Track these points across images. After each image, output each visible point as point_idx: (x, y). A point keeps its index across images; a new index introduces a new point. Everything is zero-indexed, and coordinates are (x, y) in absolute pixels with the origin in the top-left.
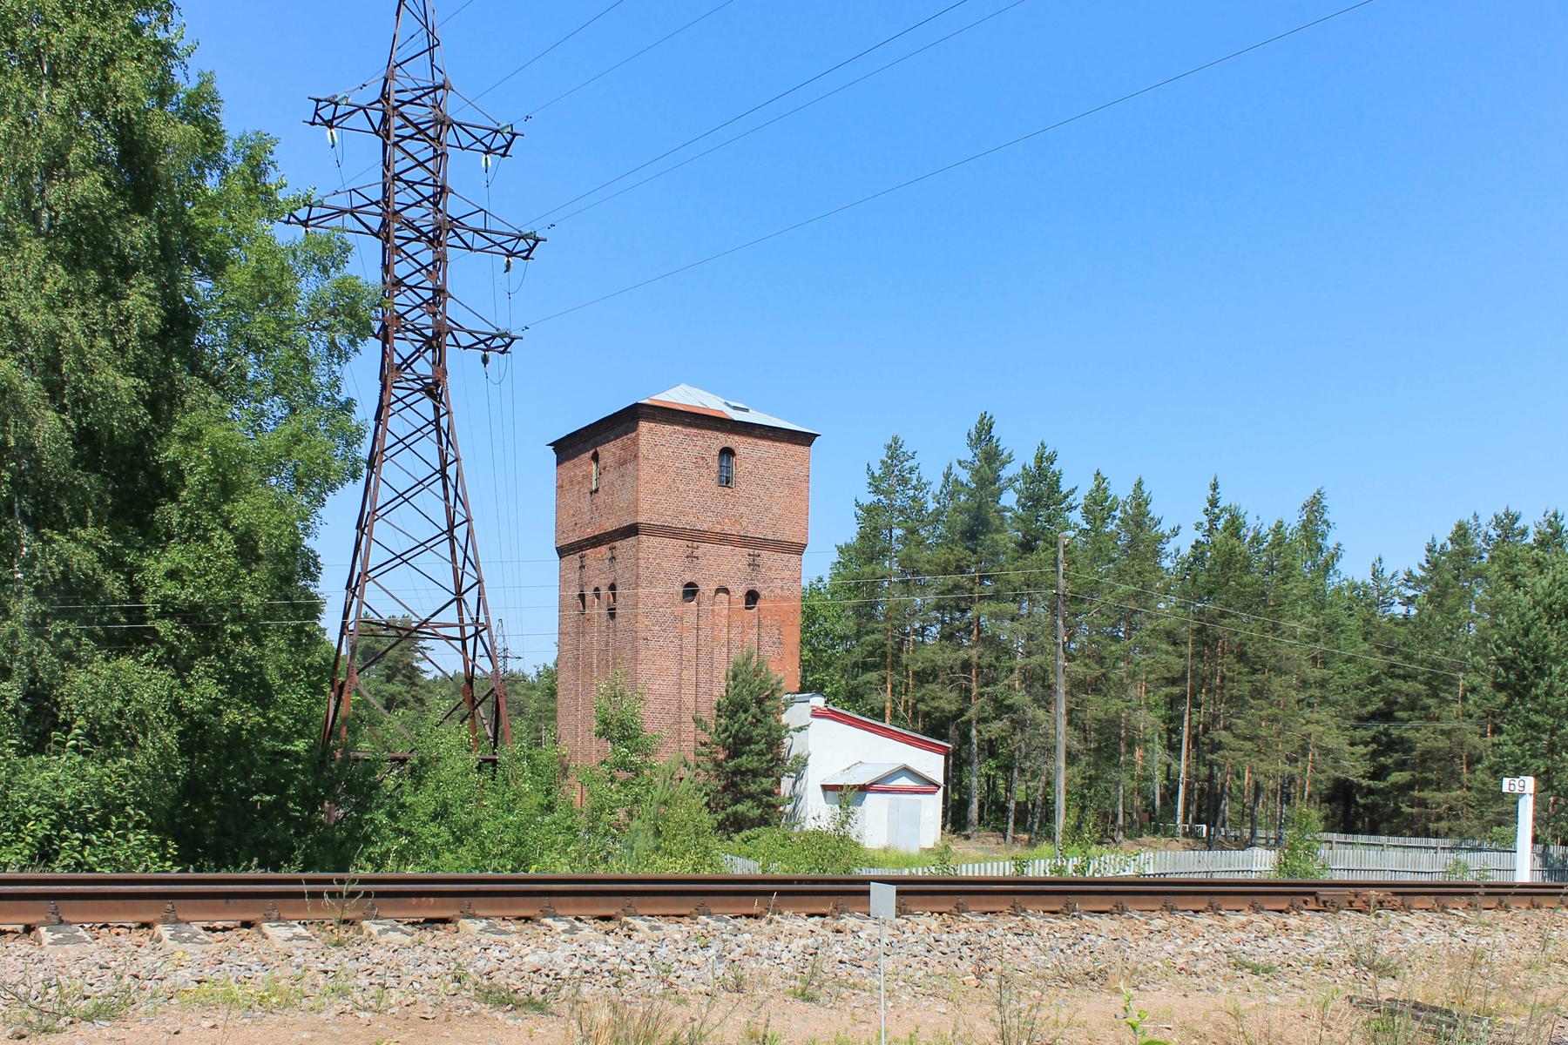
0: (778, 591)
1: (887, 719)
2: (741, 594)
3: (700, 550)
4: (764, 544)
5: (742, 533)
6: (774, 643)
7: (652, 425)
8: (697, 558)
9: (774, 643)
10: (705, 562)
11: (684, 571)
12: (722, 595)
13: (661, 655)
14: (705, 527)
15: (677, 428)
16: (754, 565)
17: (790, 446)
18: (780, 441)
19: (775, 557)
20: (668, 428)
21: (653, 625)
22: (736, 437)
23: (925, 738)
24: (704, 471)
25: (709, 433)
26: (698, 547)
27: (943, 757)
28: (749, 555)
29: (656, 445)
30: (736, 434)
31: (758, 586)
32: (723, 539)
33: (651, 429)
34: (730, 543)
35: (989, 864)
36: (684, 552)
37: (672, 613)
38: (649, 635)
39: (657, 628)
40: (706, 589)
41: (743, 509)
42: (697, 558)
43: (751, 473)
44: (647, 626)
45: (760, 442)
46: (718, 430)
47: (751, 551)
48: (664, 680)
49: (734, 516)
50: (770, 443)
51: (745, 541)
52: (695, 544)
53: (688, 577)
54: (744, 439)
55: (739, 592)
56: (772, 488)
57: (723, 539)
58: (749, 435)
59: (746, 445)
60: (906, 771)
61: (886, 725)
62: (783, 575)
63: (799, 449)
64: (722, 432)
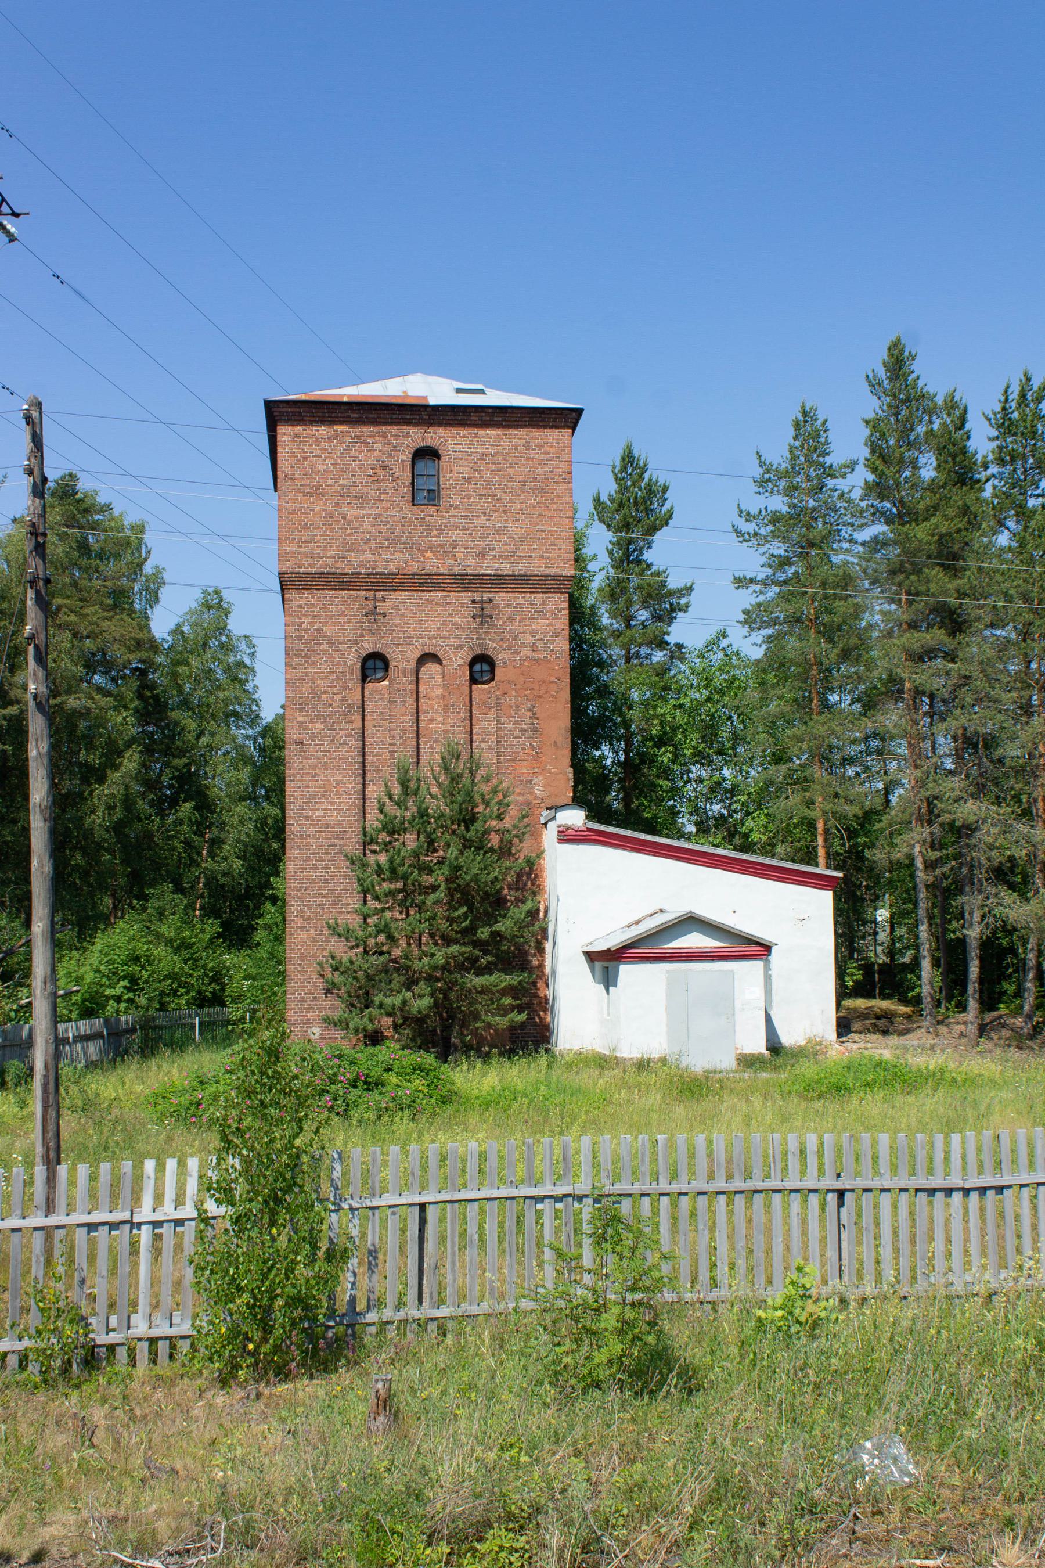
0: (527, 652)
1: (821, 860)
2: (461, 662)
3: (388, 603)
4: (499, 582)
5: (456, 570)
6: (523, 731)
7: (298, 429)
8: (384, 615)
9: (523, 731)
10: (397, 620)
11: (361, 635)
12: (431, 667)
13: (325, 765)
14: (392, 568)
15: (340, 428)
16: (483, 616)
17: (535, 432)
18: (517, 426)
19: (521, 601)
20: (324, 431)
21: (312, 721)
22: (441, 431)
23: (628, 833)
24: (389, 486)
25: (394, 429)
26: (384, 599)
27: (824, 900)
28: (474, 602)
29: (305, 458)
30: (440, 424)
31: (491, 646)
32: (425, 582)
33: (297, 436)
34: (438, 586)
35: (171, 1164)
36: (361, 608)
37: (343, 700)
38: (304, 736)
39: (319, 725)
40: (403, 659)
41: (455, 535)
42: (384, 615)
43: (468, 480)
44: (301, 724)
45: (482, 433)
46: (408, 422)
47: (477, 596)
48: (332, 803)
49: (441, 546)
50: (499, 432)
51: (464, 582)
52: (379, 595)
53: (369, 646)
54: (454, 431)
55: (458, 661)
56: (506, 498)
57: (425, 582)
58: (462, 424)
59: (459, 440)
60: (691, 922)
61: (821, 870)
62: (535, 626)
63: (554, 437)
64: (416, 425)
